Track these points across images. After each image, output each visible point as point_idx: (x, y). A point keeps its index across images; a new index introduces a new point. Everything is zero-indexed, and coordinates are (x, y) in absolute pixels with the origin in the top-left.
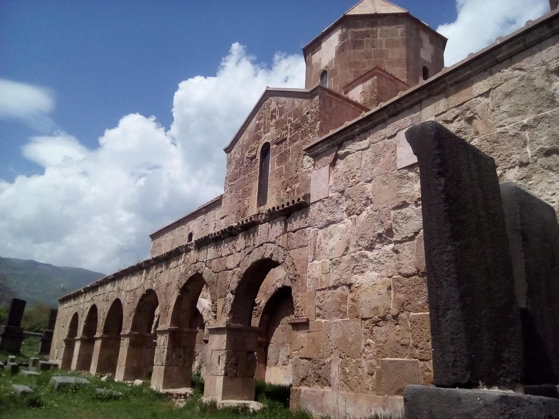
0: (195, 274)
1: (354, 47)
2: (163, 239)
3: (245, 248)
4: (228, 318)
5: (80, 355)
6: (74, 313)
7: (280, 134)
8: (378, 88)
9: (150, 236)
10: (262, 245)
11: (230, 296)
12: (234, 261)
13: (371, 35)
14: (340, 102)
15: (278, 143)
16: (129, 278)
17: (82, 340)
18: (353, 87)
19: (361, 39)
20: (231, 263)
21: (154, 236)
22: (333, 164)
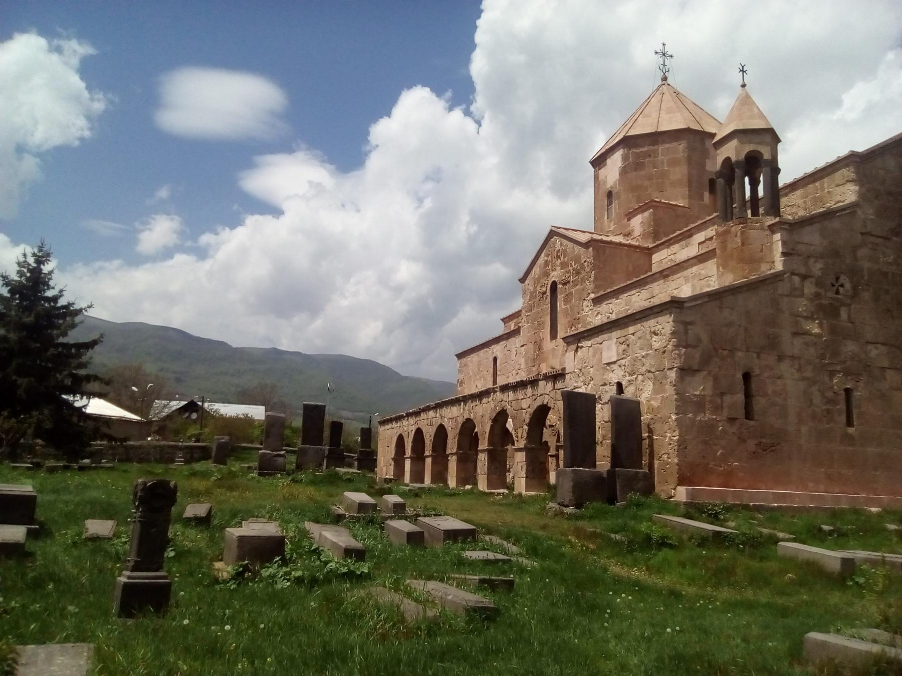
0: (502, 410)
1: (636, 170)
2: (469, 359)
4: (525, 442)
5: (411, 471)
6: (398, 434)
7: (564, 276)
8: (655, 220)
11: (526, 427)
12: (526, 403)
13: (652, 155)
14: (614, 248)
15: (564, 284)
16: (449, 407)
17: (411, 458)
21: (460, 356)
22: (576, 351)
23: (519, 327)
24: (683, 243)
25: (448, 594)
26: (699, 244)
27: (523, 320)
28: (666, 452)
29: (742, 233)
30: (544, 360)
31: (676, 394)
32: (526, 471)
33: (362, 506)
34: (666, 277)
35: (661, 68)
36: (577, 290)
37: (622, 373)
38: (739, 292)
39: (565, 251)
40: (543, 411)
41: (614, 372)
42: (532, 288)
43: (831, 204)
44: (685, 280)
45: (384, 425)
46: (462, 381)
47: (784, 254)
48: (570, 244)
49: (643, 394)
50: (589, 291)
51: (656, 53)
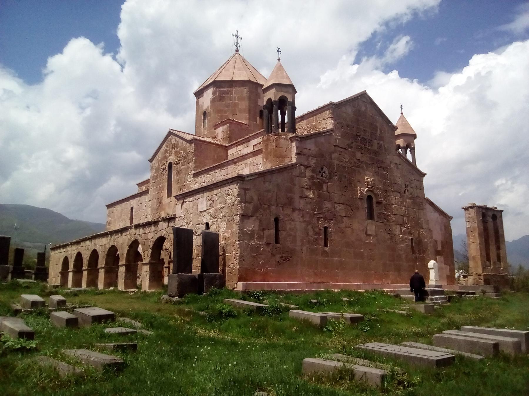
0: (135, 240)
1: (220, 100)
2: (115, 208)
3: (155, 231)
4: (150, 259)
6: (64, 256)
9: (107, 206)
10: (161, 230)
11: (150, 250)
13: (230, 93)
15: (176, 164)
17: (73, 271)
18: (218, 127)
19: (224, 95)
20: (150, 236)
21: (109, 206)
22: (183, 204)
23: (148, 190)
24: (245, 144)
25: (92, 356)
26: (254, 146)
27: (151, 185)
28: (233, 262)
29: (276, 140)
30: (163, 209)
31: (239, 229)
32: (150, 276)
33: (34, 304)
34: (235, 163)
35: (236, 44)
36: (184, 168)
37: (209, 217)
38: (274, 173)
39: (177, 144)
40: (161, 240)
41: (204, 217)
42: (156, 166)
43: (320, 129)
44: (246, 165)
45: (55, 251)
46: (109, 222)
47: (297, 154)
48: (181, 141)
49: (221, 230)
50: (191, 169)
51: (233, 35)
